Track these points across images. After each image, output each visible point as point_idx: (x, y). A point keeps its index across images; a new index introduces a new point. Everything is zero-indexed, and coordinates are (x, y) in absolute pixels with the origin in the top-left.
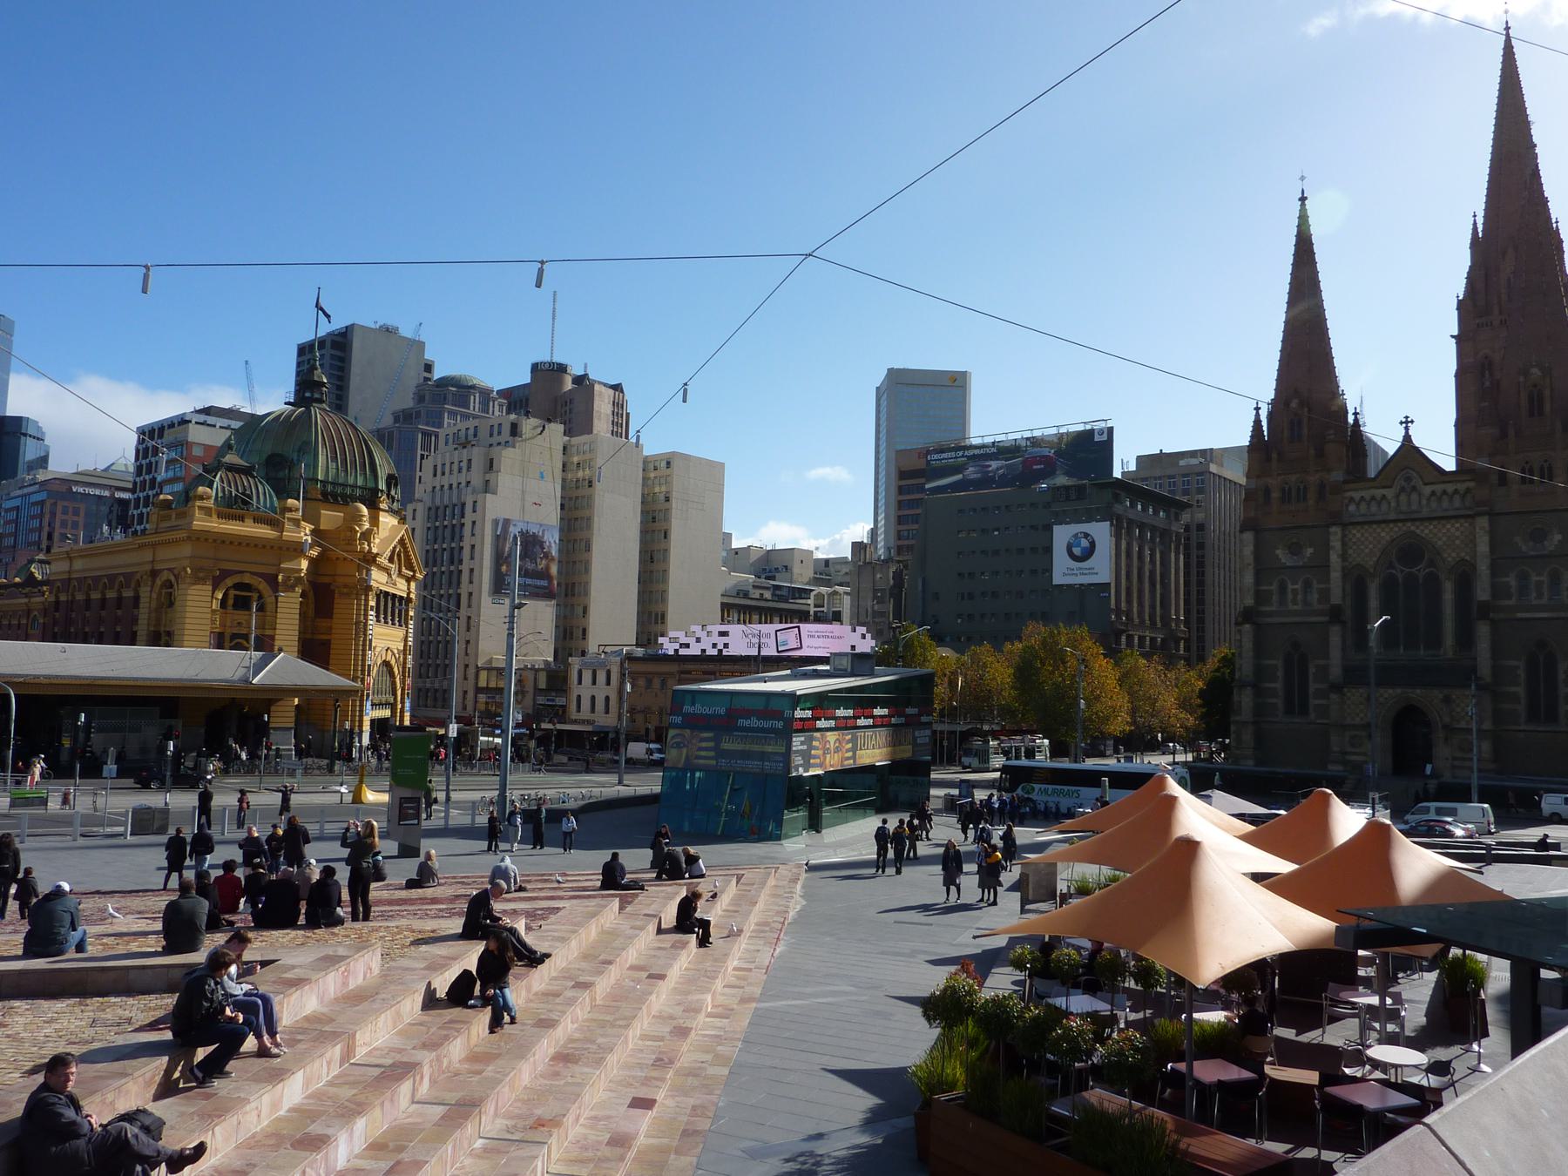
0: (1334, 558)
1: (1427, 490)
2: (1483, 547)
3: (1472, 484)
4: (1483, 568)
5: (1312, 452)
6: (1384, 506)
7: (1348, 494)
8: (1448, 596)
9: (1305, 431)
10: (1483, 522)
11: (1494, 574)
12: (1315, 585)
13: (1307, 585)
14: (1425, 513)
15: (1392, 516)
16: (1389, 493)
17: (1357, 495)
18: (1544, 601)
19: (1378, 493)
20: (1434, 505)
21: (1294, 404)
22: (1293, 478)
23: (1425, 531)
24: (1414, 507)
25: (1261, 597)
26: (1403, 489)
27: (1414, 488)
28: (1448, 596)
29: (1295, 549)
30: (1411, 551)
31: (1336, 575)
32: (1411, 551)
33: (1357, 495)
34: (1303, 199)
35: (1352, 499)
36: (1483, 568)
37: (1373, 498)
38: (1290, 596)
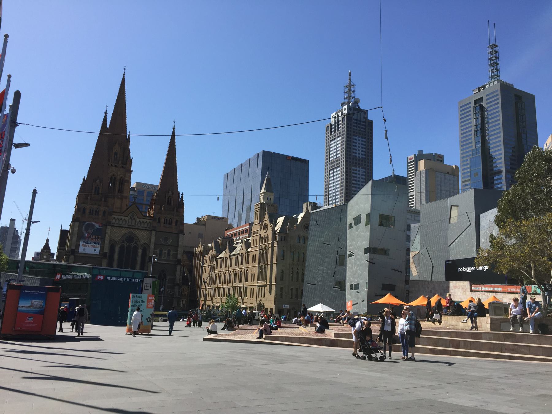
0: (107, 236)
2: (153, 240)
3: (151, 221)
4: (152, 246)
6: (124, 222)
8: (140, 254)
10: (154, 233)
11: (154, 249)
14: (136, 227)
15: (126, 226)
16: (127, 218)
17: (116, 217)
18: (165, 258)
19: (123, 218)
20: (139, 225)
21: (98, 181)
22: (95, 207)
23: (137, 232)
26: (131, 218)
27: (134, 219)
28: (140, 254)
30: (130, 238)
31: (107, 242)
32: (130, 238)
33: (116, 217)
35: (114, 218)
36: (152, 246)
37: (121, 219)
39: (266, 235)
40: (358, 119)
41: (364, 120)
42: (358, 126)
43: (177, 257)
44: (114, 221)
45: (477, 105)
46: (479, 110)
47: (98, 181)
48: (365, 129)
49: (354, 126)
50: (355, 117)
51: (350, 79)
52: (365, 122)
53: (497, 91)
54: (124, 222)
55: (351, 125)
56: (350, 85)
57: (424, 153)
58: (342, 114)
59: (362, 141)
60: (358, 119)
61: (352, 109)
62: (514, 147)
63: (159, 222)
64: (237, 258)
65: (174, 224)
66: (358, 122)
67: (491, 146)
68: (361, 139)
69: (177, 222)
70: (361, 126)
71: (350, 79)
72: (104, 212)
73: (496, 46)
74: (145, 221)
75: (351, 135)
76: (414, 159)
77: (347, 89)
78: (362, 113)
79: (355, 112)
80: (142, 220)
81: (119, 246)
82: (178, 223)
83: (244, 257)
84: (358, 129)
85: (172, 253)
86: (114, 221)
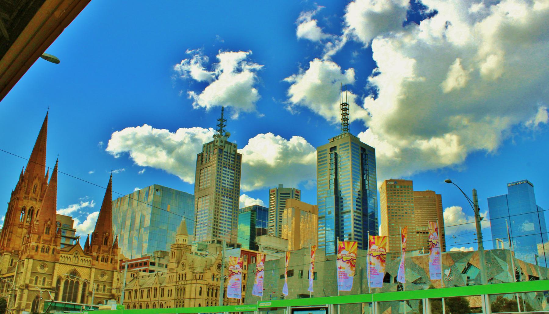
1: (81, 258)
4: (92, 281)
5: (53, 239)
6: (69, 260)
7: (61, 254)
9: (50, 232)
12: (47, 280)
13: (44, 279)
15: (71, 263)
16: (71, 257)
17: (63, 255)
19: (69, 256)
21: (49, 223)
22: (46, 246)
23: (79, 269)
24: (76, 262)
25: (31, 281)
29: (43, 267)
30: (74, 273)
32: (74, 273)
33: (63, 255)
34: (57, 161)
36: (92, 281)
38: (38, 282)
39: (184, 272)
40: (229, 152)
41: (234, 153)
42: (228, 158)
43: (111, 292)
44: (61, 258)
45: (332, 152)
46: (333, 156)
47: (49, 223)
48: (234, 161)
49: (224, 158)
50: (225, 150)
51: (222, 114)
52: (234, 155)
53: (348, 143)
54: (69, 260)
55: (222, 156)
56: (221, 119)
57: (284, 187)
58: (214, 146)
59: (231, 173)
60: (229, 152)
61: (224, 142)
62: (359, 191)
63: (97, 260)
64: (149, 291)
65: (109, 262)
66: (229, 155)
67: (343, 189)
68: (230, 171)
69: (112, 260)
70: (231, 159)
71: (222, 114)
72: (54, 250)
73: (347, 104)
74: (86, 259)
75: (221, 166)
76: (275, 192)
77: (219, 123)
78: (232, 147)
79: (226, 145)
80: (83, 258)
81: (64, 281)
82: (113, 261)
83: (158, 291)
84: (228, 161)
85: (107, 287)
86: (61, 258)
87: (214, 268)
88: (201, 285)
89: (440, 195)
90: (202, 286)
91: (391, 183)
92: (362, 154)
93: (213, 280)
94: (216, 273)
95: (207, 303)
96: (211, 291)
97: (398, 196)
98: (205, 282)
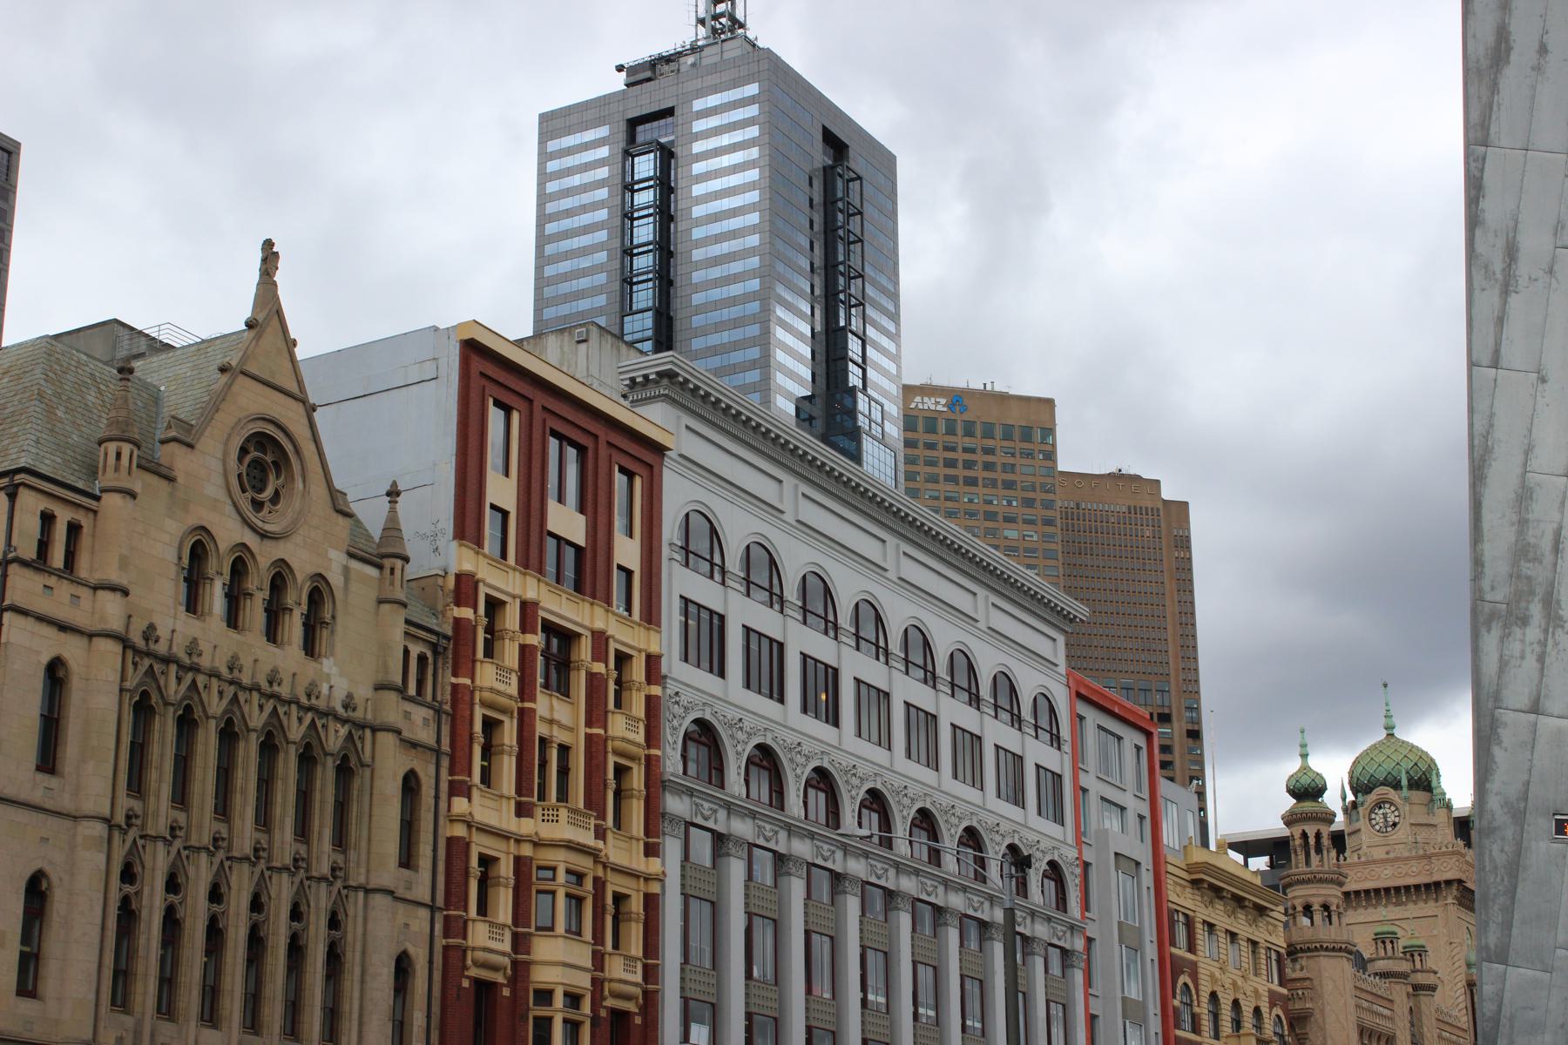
87: (208, 470)
88: (48, 644)
89: (1183, 506)
90: (71, 649)
91: (929, 403)
92: (828, 174)
93: (193, 604)
94: (229, 532)
95: (128, 875)
96: (164, 732)
97: (971, 482)
98: (111, 611)
